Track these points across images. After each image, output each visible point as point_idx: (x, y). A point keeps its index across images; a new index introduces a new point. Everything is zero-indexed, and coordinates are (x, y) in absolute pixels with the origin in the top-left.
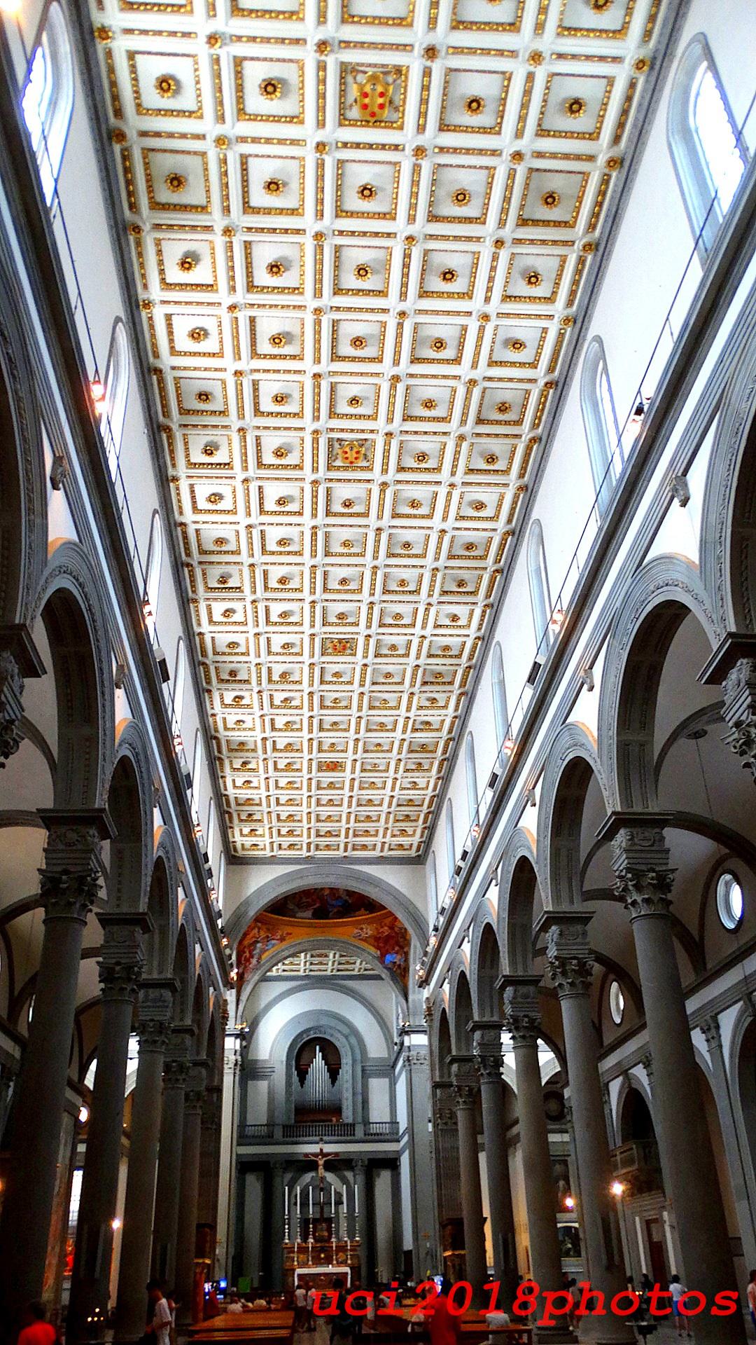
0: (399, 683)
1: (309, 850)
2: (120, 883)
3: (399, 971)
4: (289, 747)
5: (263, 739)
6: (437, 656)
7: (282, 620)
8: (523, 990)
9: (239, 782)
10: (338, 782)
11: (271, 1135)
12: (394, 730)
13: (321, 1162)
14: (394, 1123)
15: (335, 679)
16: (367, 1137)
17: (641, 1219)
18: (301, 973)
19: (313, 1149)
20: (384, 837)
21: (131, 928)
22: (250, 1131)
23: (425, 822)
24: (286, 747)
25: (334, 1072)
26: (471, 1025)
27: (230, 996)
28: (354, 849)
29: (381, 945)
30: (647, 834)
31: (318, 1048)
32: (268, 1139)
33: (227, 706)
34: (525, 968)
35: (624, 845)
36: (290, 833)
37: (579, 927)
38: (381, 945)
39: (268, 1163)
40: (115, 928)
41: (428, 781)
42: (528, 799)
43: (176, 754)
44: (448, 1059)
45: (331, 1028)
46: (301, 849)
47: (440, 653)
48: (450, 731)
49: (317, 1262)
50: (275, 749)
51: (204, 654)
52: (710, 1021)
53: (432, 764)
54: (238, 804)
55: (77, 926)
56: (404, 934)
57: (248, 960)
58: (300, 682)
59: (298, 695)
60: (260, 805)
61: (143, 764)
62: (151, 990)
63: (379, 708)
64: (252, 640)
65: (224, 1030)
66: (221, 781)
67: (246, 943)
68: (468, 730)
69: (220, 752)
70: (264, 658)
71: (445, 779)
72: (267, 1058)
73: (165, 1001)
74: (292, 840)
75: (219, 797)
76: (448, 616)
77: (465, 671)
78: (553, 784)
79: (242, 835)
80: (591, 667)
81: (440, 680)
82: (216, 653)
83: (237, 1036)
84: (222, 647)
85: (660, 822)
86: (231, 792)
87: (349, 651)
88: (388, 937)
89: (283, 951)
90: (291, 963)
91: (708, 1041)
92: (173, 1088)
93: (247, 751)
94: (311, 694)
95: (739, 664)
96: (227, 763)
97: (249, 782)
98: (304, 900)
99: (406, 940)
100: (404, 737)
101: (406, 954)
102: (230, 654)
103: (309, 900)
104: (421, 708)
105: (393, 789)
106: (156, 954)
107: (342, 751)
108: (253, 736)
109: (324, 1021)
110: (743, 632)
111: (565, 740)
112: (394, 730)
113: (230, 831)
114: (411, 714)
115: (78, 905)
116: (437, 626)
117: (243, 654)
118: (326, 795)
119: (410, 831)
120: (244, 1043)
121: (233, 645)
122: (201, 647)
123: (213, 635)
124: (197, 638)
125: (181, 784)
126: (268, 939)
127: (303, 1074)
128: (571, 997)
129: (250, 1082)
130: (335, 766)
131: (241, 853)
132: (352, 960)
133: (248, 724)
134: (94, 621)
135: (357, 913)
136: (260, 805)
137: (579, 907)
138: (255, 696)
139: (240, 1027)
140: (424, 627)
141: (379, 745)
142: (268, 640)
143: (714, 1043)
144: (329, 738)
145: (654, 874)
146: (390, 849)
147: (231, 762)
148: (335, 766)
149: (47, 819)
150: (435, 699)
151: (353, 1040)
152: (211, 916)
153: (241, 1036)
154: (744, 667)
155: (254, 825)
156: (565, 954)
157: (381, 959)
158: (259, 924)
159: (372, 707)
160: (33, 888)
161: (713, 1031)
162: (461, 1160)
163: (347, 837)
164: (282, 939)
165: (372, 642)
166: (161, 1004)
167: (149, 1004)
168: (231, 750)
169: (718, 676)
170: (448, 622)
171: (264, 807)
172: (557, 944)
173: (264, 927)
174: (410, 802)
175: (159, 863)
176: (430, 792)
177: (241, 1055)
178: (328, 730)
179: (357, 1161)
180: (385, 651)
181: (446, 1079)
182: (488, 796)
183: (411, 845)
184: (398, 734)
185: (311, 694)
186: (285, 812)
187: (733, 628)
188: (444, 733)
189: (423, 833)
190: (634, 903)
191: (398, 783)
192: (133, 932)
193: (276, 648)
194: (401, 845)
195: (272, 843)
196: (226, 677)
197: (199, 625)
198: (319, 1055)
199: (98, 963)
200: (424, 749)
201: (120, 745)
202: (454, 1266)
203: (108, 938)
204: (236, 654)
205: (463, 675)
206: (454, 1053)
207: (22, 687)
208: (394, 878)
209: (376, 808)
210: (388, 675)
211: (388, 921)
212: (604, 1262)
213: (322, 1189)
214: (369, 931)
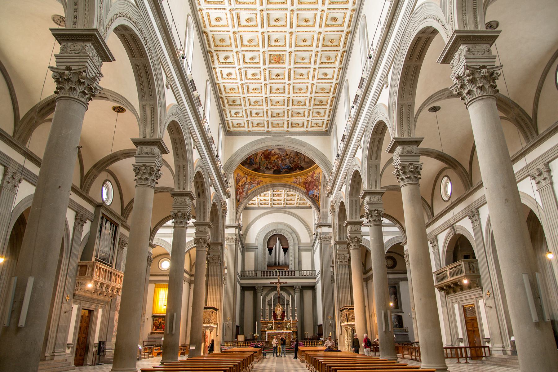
3: (316, 199)
8: (408, 148)
14: (313, 270)
16: (301, 276)
17: (459, 306)
18: (269, 206)
19: (277, 281)
20: (308, 117)
25: (285, 250)
27: (229, 203)
28: (292, 127)
29: (307, 186)
31: (278, 238)
32: (255, 277)
38: (307, 186)
39: (255, 287)
41: (332, 71)
45: (284, 230)
49: (277, 328)
54: (226, 92)
57: (242, 193)
67: (240, 184)
69: (210, 47)
71: (344, 69)
72: (254, 243)
79: (231, 116)
83: (236, 227)
86: (220, 81)
88: (311, 182)
92: (179, 227)
97: (230, 74)
99: (319, 182)
101: (319, 190)
103: (272, 166)
109: (280, 227)
113: (224, 112)
119: (322, 111)
127: (270, 250)
129: (246, 253)
130: (278, 59)
131: (232, 129)
135: (295, 171)
146: (312, 127)
147: (218, 55)
148: (278, 59)
151: (294, 235)
153: (239, 227)
157: (307, 193)
158: (246, 176)
164: (258, 184)
167: (142, 155)
168: (216, 46)
173: (249, 177)
176: (334, 81)
177: (240, 237)
179: (296, 287)
189: (330, 113)
192: (84, 48)
198: (278, 242)
203: (63, 49)
208: (314, 142)
211: (310, 174)
214: (301, 179)
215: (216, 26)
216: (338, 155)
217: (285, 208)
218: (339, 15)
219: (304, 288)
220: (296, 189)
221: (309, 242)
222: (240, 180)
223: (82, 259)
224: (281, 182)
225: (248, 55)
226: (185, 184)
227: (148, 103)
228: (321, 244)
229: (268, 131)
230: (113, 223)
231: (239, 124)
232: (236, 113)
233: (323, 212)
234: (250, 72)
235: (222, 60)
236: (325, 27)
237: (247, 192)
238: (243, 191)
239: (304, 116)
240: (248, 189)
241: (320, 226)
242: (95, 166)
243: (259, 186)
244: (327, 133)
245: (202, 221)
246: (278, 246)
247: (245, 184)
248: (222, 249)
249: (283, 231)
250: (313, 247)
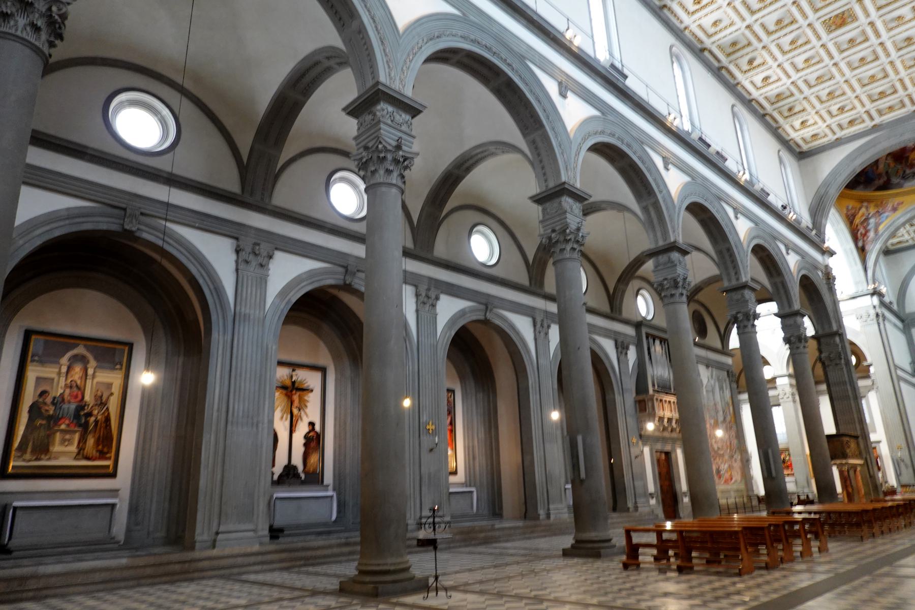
1: (872, 119)
9: (759, 82)
36: (841, 109)
57: (865, 235)
60: (792, 95)
62: (660, 257)
67: (857, 220)
69: (718, 61)
73: (673, 262)
83: (873, 294)
86: (755, 94)
89: (898, 218)
93: (744, 47)
96: (732, 68)
97: (766, 79)
98: (908, 171)
106: (658, 228)
108: (735, 30)
131: (805, 147)
136: (792, 95)
139: (873, 286)
148: (841, 20)
164: (895, 209)
166: (669, 265)
171: (797, 95)
173: (872, 205)
186: (823, 90)
195: (829, 126)
215: (716, 33)
222: (854, 216)
223: (638, 392)
225: (785, 42)
229: (875, 126)
230: (663, 341)
232: (802, 123)
235: (745, 67)
238: (867, 231)
242: (619, 280)
245: (787, 310)
247: (867, 219)
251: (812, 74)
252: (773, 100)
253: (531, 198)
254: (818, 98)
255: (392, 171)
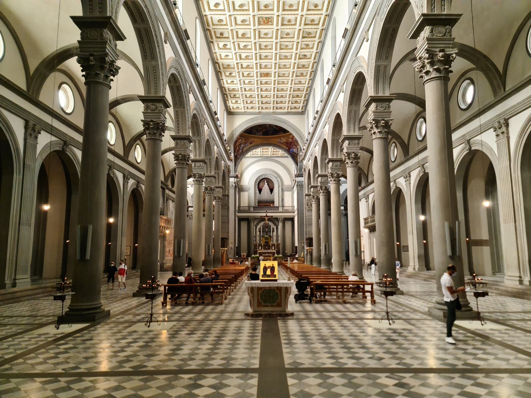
0: (292, 38)
1: (259, 109)
2: (178, 124)
4: (248, 67)
5: (237, 63)
6: (309, 24)
7: (240, 9)
8: (335, 164)
9: (229, 81)
10: (269, 81)
11: (249, 210)
12: (291, 59)
13: (267, 218)
14: (293, 206)
15: (265, 36)
18: (259, 155)
19: (264, 214)
21: (185, 141)
22: (242, 208)
23: (305, 97)
24: (247, 67)
25: (272, 190)
26: (317, 175)
30: (383, 105)
33: (221, 49)
34: (337, 156)
35: (373, 110)
36: (251, 102)
37: (356, 141)
38: (289, 145)
40: (178, 141)
42: (341, 91)
43: (197, 71)
44: (310, 186)
46: (256, 109)
47: (309, 23)
48: (315, 59)
49: (265, 249)
50: (242, 67)
51: (208, 25)
52: (407, 174)
53: (307, 73)
55: (159, 142)
56: (297, 142)
57: (238, 151)
58: (250, 38)
59: (250, 43)
61: (182, 76)
62: (196, 163)
63: (284, 49)
64: (228, 18)
65: (229, 176)
66: (221, 81)
67: (237, 144)
68: (322, 58)
69: (220, 69)
70: (234, 27)
71: (312, 80)
72: (247, 184)
74: (252, 105)
75: (222, 89)
76: (313, 4)
77: (321, 31)
78: (351, 83)
79: (232, 103)
80: (368, 31)
81: (310, 36)
82: (213, 25)
83: (235, 177)
84: (216, 22)
85: (388, 100)
86: (226, 86)
87: (270, 23)
88: (292, 142)
90: (255, 152)
91: (406, 181)
94: (255, 43)
95: (425, 29)
96: (223, 73)
97: (233, 81)
100: (295, 61)
102: (220, 25)
104: (302, 49)
105: (291, 84)
107: (270, 68)
108: (233, 62)
109: (268, 172)
110: (430, 13)
111: (356, 64)
112: (291, 59)
113: (227, 101)
114: (298, 52)
115: (158, 134)
116: (308, 10)
117: (225, 25)
118: (264, 87)
120: (238, 180)
121: (220, 21)
122: (207, 22)
123: (211, 16)
124: (205, 18)
125: (201, 84)
126: (245, 143)
127: (260, 190)
128: (351, 167)
130: (267, 75)
131: (232, 110)
132: (278, 150)
133: (230, 57)
134: (149, 12)
137: (357, 133)
138: (232, 44)
140: (302, 11)
141: (285, 65)
142: (235, 18)
143: (408, 182)
144: (264, 62)
145: (384, 122)
146: (291, 109)
147: (225, 73)
148: (267, 75)
149: (143, 100)
150: (308, 45)
151: (279, 179)
152: (221, 136)
154: (427, 31)
155: (237, 99)
156: (350, 151)
159: (281, 49)
160: (140, 128)
161: (408, 178)
162: (313, 220)
163: (274, 104)
164: (251, 143)
165: (280, 18)
167: (196, 168)
168: (224, 68)
169: (415, 35)
170: (313, 8)
172: (347, 148)
174: (299, 90)
175: (194, 115)
176: (306, 85)
177: (237, 184)
178: (264, 59)
180: (286, 23)
181: (310, 193)
182: (327, 88)
183: (299, 107)
184: (293, 61)
185: (255, 43)
186: (248, 94)
187: (425, 11)
188: (312, 60)
190: (374, 133)
191: (293, 82)
193: (239, 22)
194: (296, 107)
195: (244, 107)
196: (219, 36)
197: (205, 11)
198: (266, 184)
199: (173, 154)
200: (304, 66)
201: (170, 69)
202: (309, 252)
203: (177, 144)
204: (222, 25)
205: (320, 33)
206: (312, 185)
207: (116, 45)
209: (285, 92)
210: (288, 34)
212: (354, 254)
213: (267, 227)
214: (284, 140)
215: (224, 59)
216: (309, 133)
217: (272, 157)
218: (308, 54)
219: (285, 219)
220: (280, 147)
221: (290, 184)
224: (268, 142)
226: (210, 170)
227: (180, 110)
228: (298, 190)
231: (238, 107)
233: (300, 166)
234: (239, 19)
236: (298, 59)
237: (242, 151)
238: (240, 149)
239: (285, 103)
240: (244, 148)
241: (297, 177)
243: (252, 145)
244: (303, 113)
246: (266, 188)
247: (240, 145)
248: (228, 198)
249: (270, 176)
250: (293, 188)
251: (248, 87)
252: (230, 90)
253: (171, 136)
254: (246, 96)
255: (156, 133)
